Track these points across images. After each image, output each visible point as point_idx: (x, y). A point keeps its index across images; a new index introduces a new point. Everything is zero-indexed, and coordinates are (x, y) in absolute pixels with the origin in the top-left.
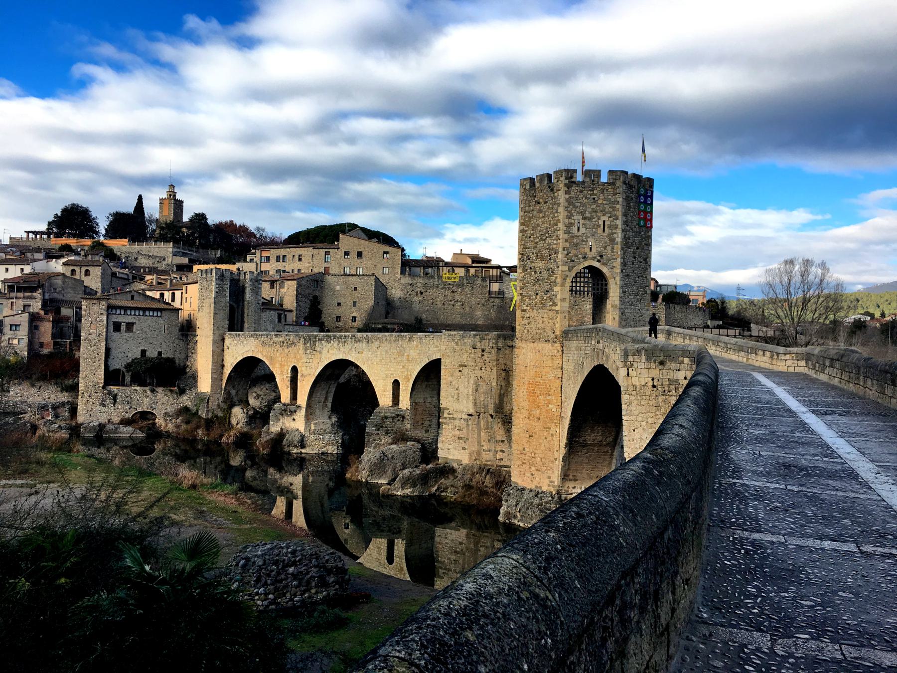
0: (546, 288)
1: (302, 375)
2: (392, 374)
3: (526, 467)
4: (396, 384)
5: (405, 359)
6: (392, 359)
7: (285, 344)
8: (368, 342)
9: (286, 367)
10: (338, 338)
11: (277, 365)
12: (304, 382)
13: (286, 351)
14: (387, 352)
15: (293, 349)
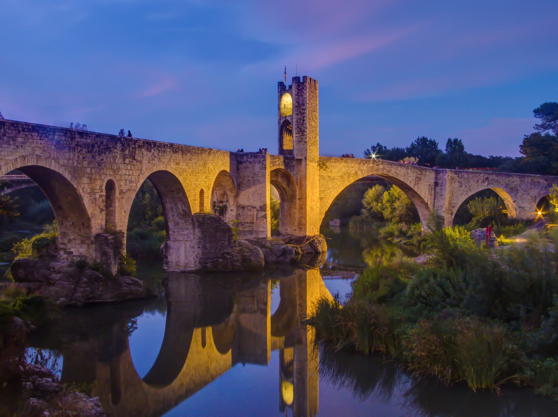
0: (315, 136)
1: (121, 192)
2: (199, 184)
3: (311, 226)
4: (202, 192)
5: (207, 171)
6: (200, 170)
7: (96, 149)
8: (183, 154)
9: (98, 183)
10: (159, 146)
11: (85, 180)
12: (124, 201)
13: (98, 158)
14: (196, 164)
15: (107, 158)
